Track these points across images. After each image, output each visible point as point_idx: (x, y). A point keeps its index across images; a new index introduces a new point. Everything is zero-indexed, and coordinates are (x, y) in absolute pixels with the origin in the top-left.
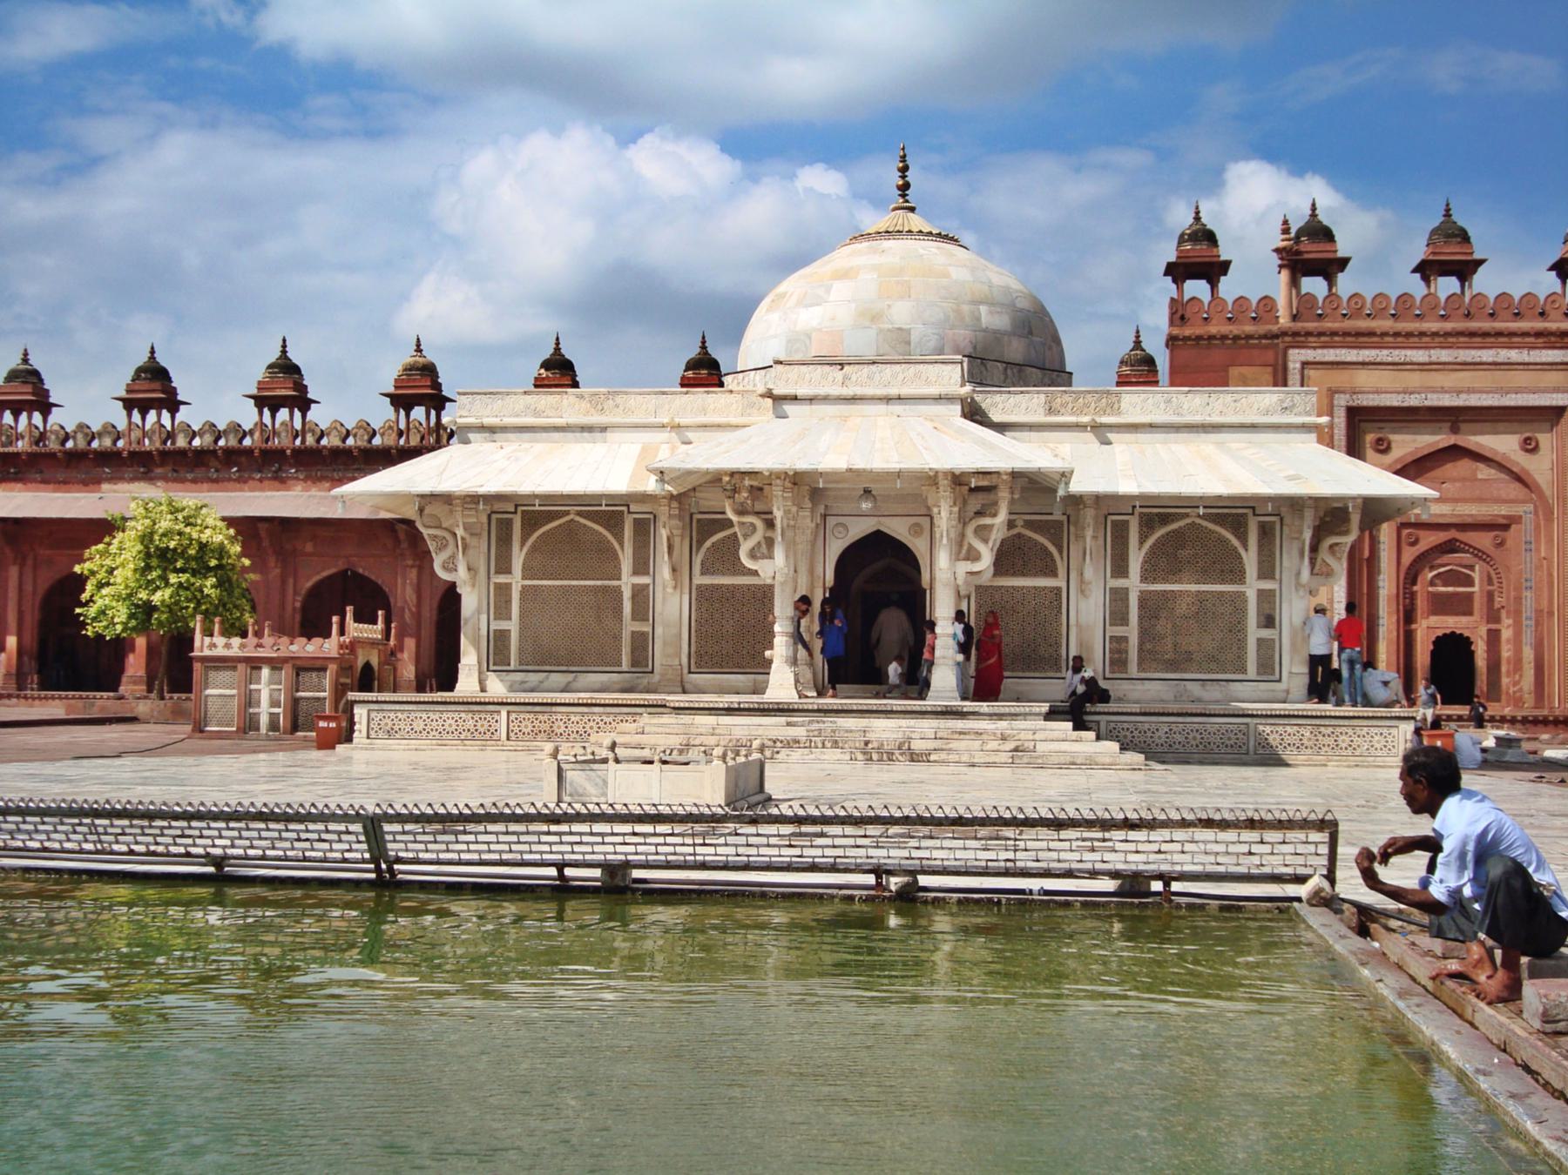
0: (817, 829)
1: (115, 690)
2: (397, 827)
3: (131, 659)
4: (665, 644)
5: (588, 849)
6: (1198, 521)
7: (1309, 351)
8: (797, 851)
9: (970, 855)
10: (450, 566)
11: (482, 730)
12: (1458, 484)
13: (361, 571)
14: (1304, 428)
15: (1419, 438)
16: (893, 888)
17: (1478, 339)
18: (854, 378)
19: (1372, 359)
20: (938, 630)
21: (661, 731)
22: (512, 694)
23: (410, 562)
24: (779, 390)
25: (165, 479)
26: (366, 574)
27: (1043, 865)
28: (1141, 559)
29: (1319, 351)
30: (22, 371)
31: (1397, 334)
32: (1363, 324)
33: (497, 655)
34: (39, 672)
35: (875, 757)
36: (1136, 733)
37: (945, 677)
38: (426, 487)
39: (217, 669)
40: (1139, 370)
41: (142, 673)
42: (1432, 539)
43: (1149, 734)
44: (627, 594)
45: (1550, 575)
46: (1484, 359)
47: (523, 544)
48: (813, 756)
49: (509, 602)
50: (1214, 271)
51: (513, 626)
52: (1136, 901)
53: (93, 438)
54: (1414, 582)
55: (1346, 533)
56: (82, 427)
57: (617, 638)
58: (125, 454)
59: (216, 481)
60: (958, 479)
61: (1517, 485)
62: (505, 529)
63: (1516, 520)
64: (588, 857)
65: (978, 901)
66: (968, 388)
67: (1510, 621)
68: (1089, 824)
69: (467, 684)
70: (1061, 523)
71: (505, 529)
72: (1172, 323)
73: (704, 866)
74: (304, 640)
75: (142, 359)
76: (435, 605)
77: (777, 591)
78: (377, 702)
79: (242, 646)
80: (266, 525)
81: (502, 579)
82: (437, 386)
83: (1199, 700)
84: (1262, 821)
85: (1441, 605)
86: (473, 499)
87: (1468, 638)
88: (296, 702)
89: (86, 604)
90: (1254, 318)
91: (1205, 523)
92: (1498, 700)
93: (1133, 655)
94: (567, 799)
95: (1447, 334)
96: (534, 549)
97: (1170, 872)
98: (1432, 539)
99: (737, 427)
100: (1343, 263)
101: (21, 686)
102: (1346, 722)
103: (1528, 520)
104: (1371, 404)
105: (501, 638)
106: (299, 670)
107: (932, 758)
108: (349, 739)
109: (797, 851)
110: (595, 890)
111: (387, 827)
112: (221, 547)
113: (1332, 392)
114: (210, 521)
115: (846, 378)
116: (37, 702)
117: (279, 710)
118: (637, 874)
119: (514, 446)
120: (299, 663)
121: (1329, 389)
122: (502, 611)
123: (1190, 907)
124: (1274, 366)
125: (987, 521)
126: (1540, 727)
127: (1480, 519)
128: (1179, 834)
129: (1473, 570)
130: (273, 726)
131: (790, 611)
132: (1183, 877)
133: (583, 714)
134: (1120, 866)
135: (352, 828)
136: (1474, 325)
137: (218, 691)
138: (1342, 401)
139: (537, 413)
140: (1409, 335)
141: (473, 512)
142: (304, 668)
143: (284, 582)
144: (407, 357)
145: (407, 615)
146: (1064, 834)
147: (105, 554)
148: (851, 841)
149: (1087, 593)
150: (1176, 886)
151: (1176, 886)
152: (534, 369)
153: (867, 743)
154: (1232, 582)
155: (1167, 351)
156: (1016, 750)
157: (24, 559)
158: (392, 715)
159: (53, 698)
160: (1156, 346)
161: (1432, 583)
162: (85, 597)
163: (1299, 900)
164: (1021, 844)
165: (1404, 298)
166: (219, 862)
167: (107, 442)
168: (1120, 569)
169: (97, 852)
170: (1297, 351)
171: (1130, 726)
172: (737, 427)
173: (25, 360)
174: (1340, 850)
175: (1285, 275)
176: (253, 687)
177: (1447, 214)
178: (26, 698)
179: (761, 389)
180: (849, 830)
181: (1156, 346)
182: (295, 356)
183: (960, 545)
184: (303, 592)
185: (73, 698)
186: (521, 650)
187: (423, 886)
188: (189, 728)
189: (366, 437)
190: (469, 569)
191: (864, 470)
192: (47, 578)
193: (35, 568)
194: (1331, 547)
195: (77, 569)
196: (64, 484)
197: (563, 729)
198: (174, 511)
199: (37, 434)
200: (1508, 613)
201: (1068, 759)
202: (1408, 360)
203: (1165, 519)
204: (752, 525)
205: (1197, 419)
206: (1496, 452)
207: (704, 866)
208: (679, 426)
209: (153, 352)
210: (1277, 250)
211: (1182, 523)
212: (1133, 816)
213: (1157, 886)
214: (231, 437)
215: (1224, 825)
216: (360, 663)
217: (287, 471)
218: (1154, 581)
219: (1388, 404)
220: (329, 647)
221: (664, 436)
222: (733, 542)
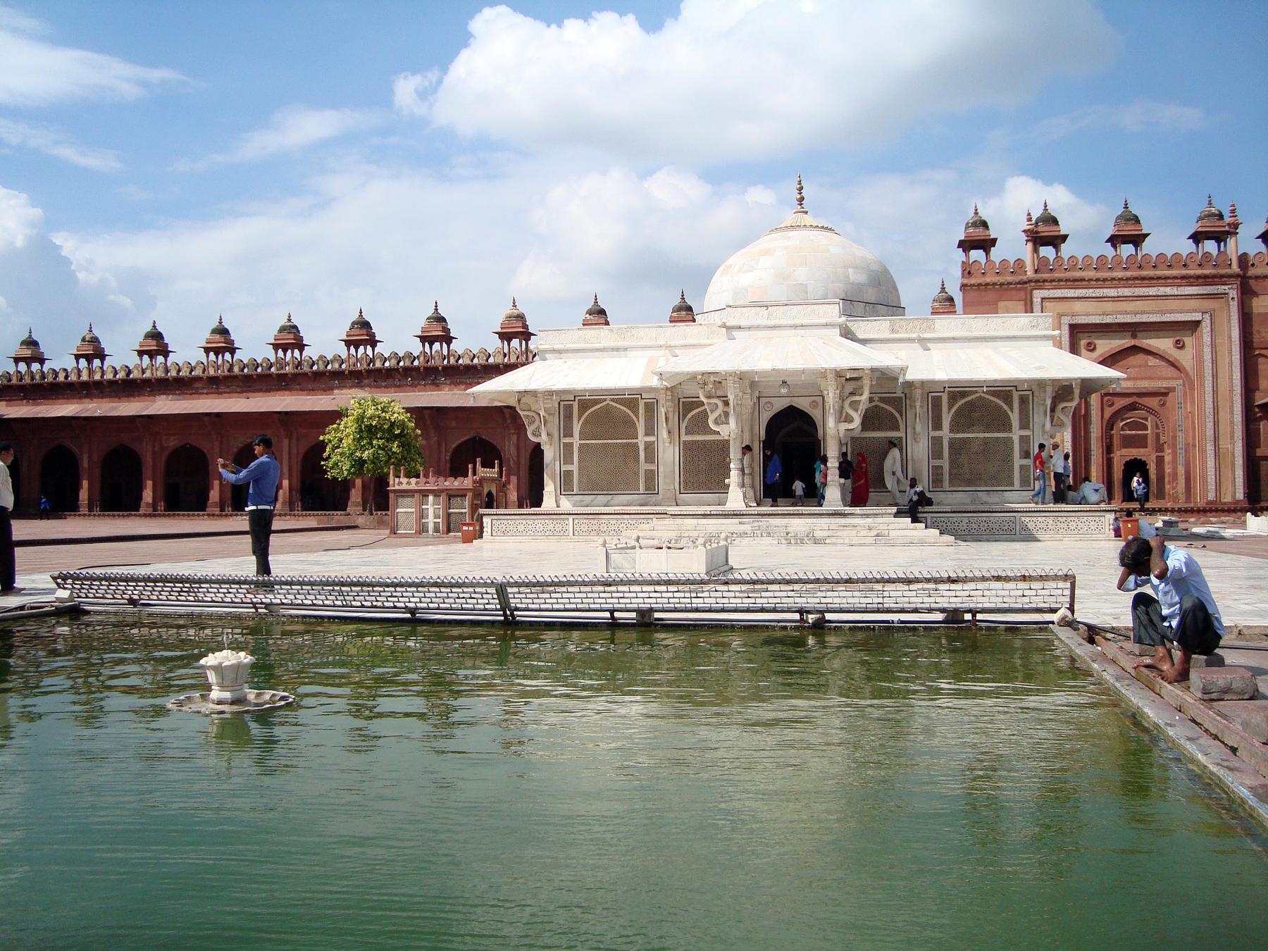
0: (764, 586)
1: (345, 510)
2: (516, 590)
3: (353, 492)
4: (665, 477)
5: (628, 601)
8: (753, 600)
9: (857, 600)
10: (537, 433)
11: (558, 530)
12: (1137, 369)
14: (1045, 337)
15: (1113, 341)
16: (810, 621)
17: (1147, 282)
18: (775, 314)
20: (829, 465)
21: (664, 529)
22: (575, 508)
23: (513, 431)
24: (727, 324)
25: (369, 386)
26: (487, 439)
27: (900, 606)
29: (1052, 291)
30: (287, 326)
31: (1098, 280)
32: (1078, 274)
33: (566, 484)
34: (302, 500)
35: (793, 542)
36: (949, 524)
37: (833, 494)
38: (521, 388)
39: (403, 496)
40: (945, 304)
41: (359, 500)
42: (1121, 403)
43: (957, 524)
44: (642, 447)
45: (1193, 422)
46: (1151, 294)
48: (755, 542)
50: (986, 244)
51: (574, 467)
52: (956, 625)
53: (328, 363)
54: (1112, 429)
55: (1072, 400)
56: (322, 357)
57: (637, 474)
58: (347, 372)
59: (399, 386)
60: (839, 374)
61: (1173, 368)
63: (1172, 390)
64: (628, 606)
65: (861, 628)
66: (843, 319)
67: (1170, 451)
68: (928, 580)
69: (548, 502)
70: (901, 398)
72: (963, 276)
73: (697, 610)
74: (453, 479)
75: (355, 317)
76: (528, 456)
77: (731, 442)
78: (496, 514)
79: (417, 483)
80: (426, 412)
81: (567, 440)
82: (525, 326)
83: (986, 503)
84: (1030, 577)
85: (1129, 442)
86: (550, 393)
87: (1145, 461)
88: (449, 515)
89: (326, 459)
90: (1012, 272)
91: (987, 396)
92: (1164, 499)
93: (946, 477)
94: (611, 570)
95: (1128, 279)
96: (586, 420)
97: (976, 608)
98: (1121, 403)
99: (705, 346)
100: (1064, 238)
101: (291, 511)
102: (1074, 514)
103: (1180, 389)
104: (1083, 322)
105: (568, 474)
106: (450, 497)
107: (827, 542)
108: (481, 537)
109: (753, 600)
110: (633, 625)
111: (509, 590)
112: (403, 425)
113: (1060, 316)
114: (396, 409)
115: (769, 315)
116: (301, 518)
117: (440, 520)
118: (657, 615)
120: (450, 492)
121: (1058, 314)
122: (568, 459)
123: (988, 628)
124: (1025, 300)
125: (857, 398)
126: (1189, 514)
127: (1150, 390)
128: (981, 585)
129: (1147, 421)
130: (436, 530)
131: (739, 455)
132: (983, 611)
133: (617, 519)
134: (946, 605)
135: (489, 590)
136: (1144, 273)
137: (404, 510)
138: (1066, 321)
139: (585, 341)
140: (1105, 280)
142: (452, 495)
143: (439, 445)
144: (508, 310)
145: (512, 462)
146: (913, 587)
147: (337, 430)
148: (784, 594)
149: (918, 440)
150: (979, 617)
151: (979, 617)
152: (582, 315)
153: (787, 534)
154: (1006, 432)
155: (961, 293)
156: (877, 536)
157: (291, 435)
158: (505, 522)
159: (310, 515)
160: (954, 291)
161: (1122, 429)
162: (325, 455)
163: (1053, 623)
164: (886, 594)
165: (1102, 258)
166: (413, 611)
167: (336, 366)
168: (937, 425)
169: (343, 606)
171: (946, 520)
172: (705, 346)
173: (289, 320)
174: (1077, 592)
175: (1030, 245)
176: (424, 507)
177: (1126, 207)
178: (294, 515)
179: (719, 323)
180: (784, 587)
181: (954, 291)
182: (442, 312)
183: (841, 413)
184: (451, 450)
185: (321, 515)
186: (580, 481)
187: (532, 625)
188: (388, 532)
189: (485, 358)
191: (782, 370)
192: (305, 446)
193: (298, 440)
195: (321, 438)
196: (313, 391)
197: (606, 528)
198: (375, 404)
199: (297, 363)
200: (1169, 445)
201: (909, 541)
202: (1105, 295)
203: (963, 394)
205: (982, 334)
206: (1159, 349)
207: (697, 610)
208: (670, 346)
209: (361, 313)
210: (1024, 231)
211: (973, 397)
212: (953, 575)
213: (968, 617)
214: (407, 360)
215: (1007, 579)
216: (486, 491)
217: (439, 380)
218: (958, 432)
219: (1094, 322)
220: (467, 482)
221: (661, 352)
222: (705, 415)
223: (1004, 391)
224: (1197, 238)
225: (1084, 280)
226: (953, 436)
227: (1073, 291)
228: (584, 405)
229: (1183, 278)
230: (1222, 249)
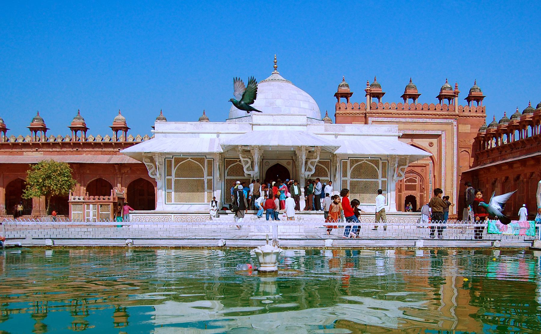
6: (366, 161)
13: (104, 179)
14: (395, 136)
19: (391, 121)
23: (119, 176)
26: (105, 179)
28: (350, 172)
29: (377, 118)
44: (206, 181)
46: (420, 121)
47: (175, 168)
55: (405, 165)
70: (329, 162)
80: (75, 165)
81: (169, 177)
86: (161, 154)
91: (368, 162)
96: (178, 168)
100: (383, 94)
115: (274, 120)
127: (418, 165)
141: (160, 158)
168: (345, 175)
170: (371, 118)
184: (87, 185)
186: (175, 198)
190: (160, 175)
194: (401, 169)
203: (357, 161)
204: (247, 162)
211: (361, 162)
218: (354, 178)
223: (376, 160)
224: (440, 97)
225: (392, 114)
226: (352, 180)
227: (386, 118)
228: (177, 161)
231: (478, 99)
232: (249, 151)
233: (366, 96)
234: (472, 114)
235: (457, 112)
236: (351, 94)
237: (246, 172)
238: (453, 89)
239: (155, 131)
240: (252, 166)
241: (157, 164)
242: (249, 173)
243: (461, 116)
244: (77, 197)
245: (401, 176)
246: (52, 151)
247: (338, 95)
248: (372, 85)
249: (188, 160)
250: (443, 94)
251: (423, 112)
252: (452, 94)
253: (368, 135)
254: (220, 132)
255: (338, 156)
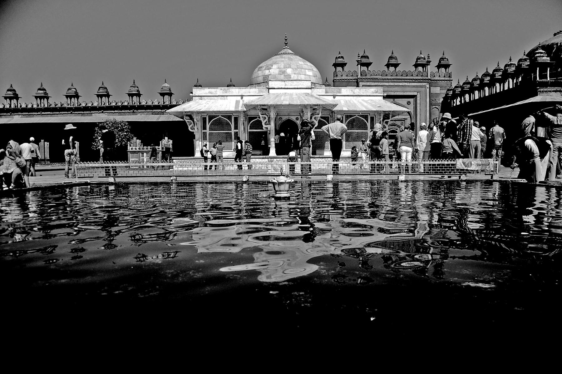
6: (358, 116)
7: (364, 83)
14: (380, 96)
49: (206, 136)
50: (343, 65)
55: (389, 119)
62: (204, 120)
70: (329, 117)
71: (204, 120)
81: (204, 131)
86: (198, 113)
91: (359, 117)
96: (212, 124)
115: (286, 85)
119: (207, 100)
139: (211, 93)
154: (365, 130)
161: (389, 133)
203: (351, 116)
224: (416, 66)
228: (211, 118)
229: (411, 80)
230: (424, 70)
231: (447, 66)
232: (266, 109)
233: (357, 65)
234: (441, 79)
235: (429, 77)
236: (346, 64)
237: (264, 126)
238: (426, 59)
239: (193, 95)
240: (269, 121)
241: (195, 120)
242: (266, 126)
243: (433, 80)
244: (134, 148)
245: (385, 128)
246: (115, 113)
247: (336, 65)
248: (362, 57)
249: (219, 117)
250: (418, 63)
251: (403, 77)
252: (425, 63)
253: (359, 96)
254: (244, 95)
255: (335, 112)
